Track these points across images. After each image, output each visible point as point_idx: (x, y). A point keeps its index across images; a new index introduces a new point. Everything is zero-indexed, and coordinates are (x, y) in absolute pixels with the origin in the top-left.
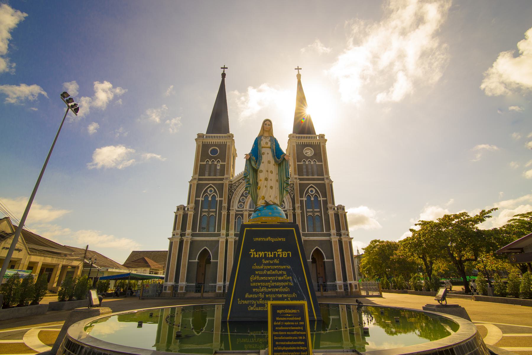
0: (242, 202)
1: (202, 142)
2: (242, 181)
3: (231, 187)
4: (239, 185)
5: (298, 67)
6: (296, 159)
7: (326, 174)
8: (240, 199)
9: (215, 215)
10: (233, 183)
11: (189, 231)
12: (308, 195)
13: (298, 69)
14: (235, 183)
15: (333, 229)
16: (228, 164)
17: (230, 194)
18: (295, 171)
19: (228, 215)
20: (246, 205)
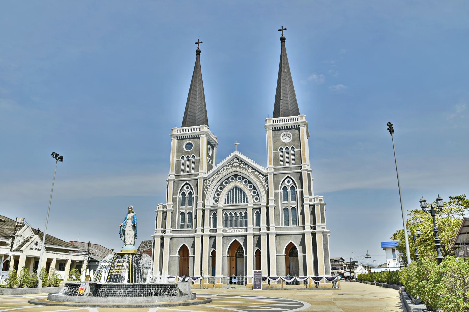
0: (217, 198)
1: (176, 138)
2: (217, 176)
3: (206, 183)
4: (213, 181)
5: (282, 27)
6: (271, 147)
7: (303, 162)
8: (215, 195)
9: (191, 212)
10: (208, 178)
11: (168, 228)
12: (285, 186)
13: (282, 30)
14: (210, 178)
15: (308, 222)
16: (202, 158)
17: (205, 191)
18: (271, 161)
19: (203, 211)
20: (221, 201)
